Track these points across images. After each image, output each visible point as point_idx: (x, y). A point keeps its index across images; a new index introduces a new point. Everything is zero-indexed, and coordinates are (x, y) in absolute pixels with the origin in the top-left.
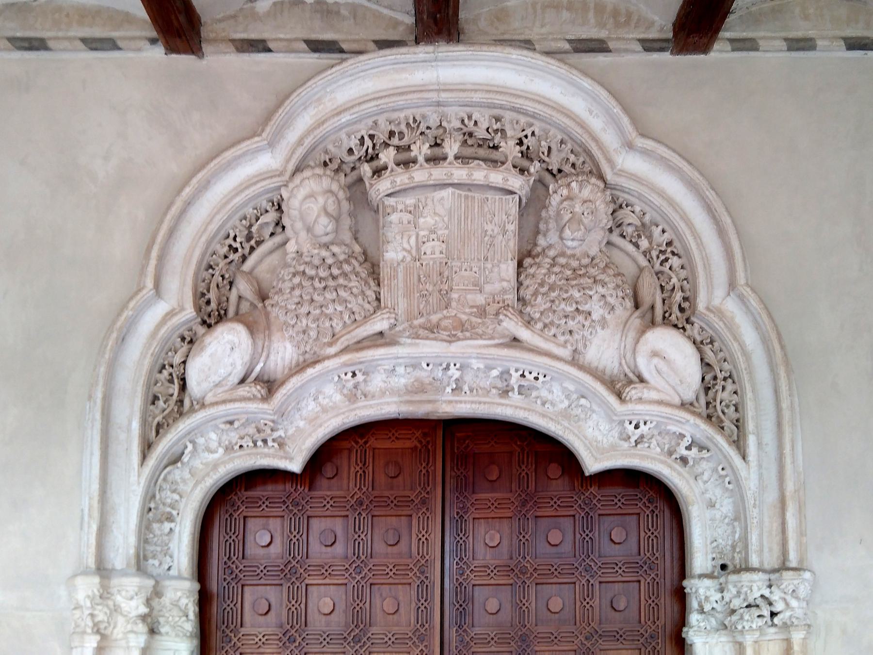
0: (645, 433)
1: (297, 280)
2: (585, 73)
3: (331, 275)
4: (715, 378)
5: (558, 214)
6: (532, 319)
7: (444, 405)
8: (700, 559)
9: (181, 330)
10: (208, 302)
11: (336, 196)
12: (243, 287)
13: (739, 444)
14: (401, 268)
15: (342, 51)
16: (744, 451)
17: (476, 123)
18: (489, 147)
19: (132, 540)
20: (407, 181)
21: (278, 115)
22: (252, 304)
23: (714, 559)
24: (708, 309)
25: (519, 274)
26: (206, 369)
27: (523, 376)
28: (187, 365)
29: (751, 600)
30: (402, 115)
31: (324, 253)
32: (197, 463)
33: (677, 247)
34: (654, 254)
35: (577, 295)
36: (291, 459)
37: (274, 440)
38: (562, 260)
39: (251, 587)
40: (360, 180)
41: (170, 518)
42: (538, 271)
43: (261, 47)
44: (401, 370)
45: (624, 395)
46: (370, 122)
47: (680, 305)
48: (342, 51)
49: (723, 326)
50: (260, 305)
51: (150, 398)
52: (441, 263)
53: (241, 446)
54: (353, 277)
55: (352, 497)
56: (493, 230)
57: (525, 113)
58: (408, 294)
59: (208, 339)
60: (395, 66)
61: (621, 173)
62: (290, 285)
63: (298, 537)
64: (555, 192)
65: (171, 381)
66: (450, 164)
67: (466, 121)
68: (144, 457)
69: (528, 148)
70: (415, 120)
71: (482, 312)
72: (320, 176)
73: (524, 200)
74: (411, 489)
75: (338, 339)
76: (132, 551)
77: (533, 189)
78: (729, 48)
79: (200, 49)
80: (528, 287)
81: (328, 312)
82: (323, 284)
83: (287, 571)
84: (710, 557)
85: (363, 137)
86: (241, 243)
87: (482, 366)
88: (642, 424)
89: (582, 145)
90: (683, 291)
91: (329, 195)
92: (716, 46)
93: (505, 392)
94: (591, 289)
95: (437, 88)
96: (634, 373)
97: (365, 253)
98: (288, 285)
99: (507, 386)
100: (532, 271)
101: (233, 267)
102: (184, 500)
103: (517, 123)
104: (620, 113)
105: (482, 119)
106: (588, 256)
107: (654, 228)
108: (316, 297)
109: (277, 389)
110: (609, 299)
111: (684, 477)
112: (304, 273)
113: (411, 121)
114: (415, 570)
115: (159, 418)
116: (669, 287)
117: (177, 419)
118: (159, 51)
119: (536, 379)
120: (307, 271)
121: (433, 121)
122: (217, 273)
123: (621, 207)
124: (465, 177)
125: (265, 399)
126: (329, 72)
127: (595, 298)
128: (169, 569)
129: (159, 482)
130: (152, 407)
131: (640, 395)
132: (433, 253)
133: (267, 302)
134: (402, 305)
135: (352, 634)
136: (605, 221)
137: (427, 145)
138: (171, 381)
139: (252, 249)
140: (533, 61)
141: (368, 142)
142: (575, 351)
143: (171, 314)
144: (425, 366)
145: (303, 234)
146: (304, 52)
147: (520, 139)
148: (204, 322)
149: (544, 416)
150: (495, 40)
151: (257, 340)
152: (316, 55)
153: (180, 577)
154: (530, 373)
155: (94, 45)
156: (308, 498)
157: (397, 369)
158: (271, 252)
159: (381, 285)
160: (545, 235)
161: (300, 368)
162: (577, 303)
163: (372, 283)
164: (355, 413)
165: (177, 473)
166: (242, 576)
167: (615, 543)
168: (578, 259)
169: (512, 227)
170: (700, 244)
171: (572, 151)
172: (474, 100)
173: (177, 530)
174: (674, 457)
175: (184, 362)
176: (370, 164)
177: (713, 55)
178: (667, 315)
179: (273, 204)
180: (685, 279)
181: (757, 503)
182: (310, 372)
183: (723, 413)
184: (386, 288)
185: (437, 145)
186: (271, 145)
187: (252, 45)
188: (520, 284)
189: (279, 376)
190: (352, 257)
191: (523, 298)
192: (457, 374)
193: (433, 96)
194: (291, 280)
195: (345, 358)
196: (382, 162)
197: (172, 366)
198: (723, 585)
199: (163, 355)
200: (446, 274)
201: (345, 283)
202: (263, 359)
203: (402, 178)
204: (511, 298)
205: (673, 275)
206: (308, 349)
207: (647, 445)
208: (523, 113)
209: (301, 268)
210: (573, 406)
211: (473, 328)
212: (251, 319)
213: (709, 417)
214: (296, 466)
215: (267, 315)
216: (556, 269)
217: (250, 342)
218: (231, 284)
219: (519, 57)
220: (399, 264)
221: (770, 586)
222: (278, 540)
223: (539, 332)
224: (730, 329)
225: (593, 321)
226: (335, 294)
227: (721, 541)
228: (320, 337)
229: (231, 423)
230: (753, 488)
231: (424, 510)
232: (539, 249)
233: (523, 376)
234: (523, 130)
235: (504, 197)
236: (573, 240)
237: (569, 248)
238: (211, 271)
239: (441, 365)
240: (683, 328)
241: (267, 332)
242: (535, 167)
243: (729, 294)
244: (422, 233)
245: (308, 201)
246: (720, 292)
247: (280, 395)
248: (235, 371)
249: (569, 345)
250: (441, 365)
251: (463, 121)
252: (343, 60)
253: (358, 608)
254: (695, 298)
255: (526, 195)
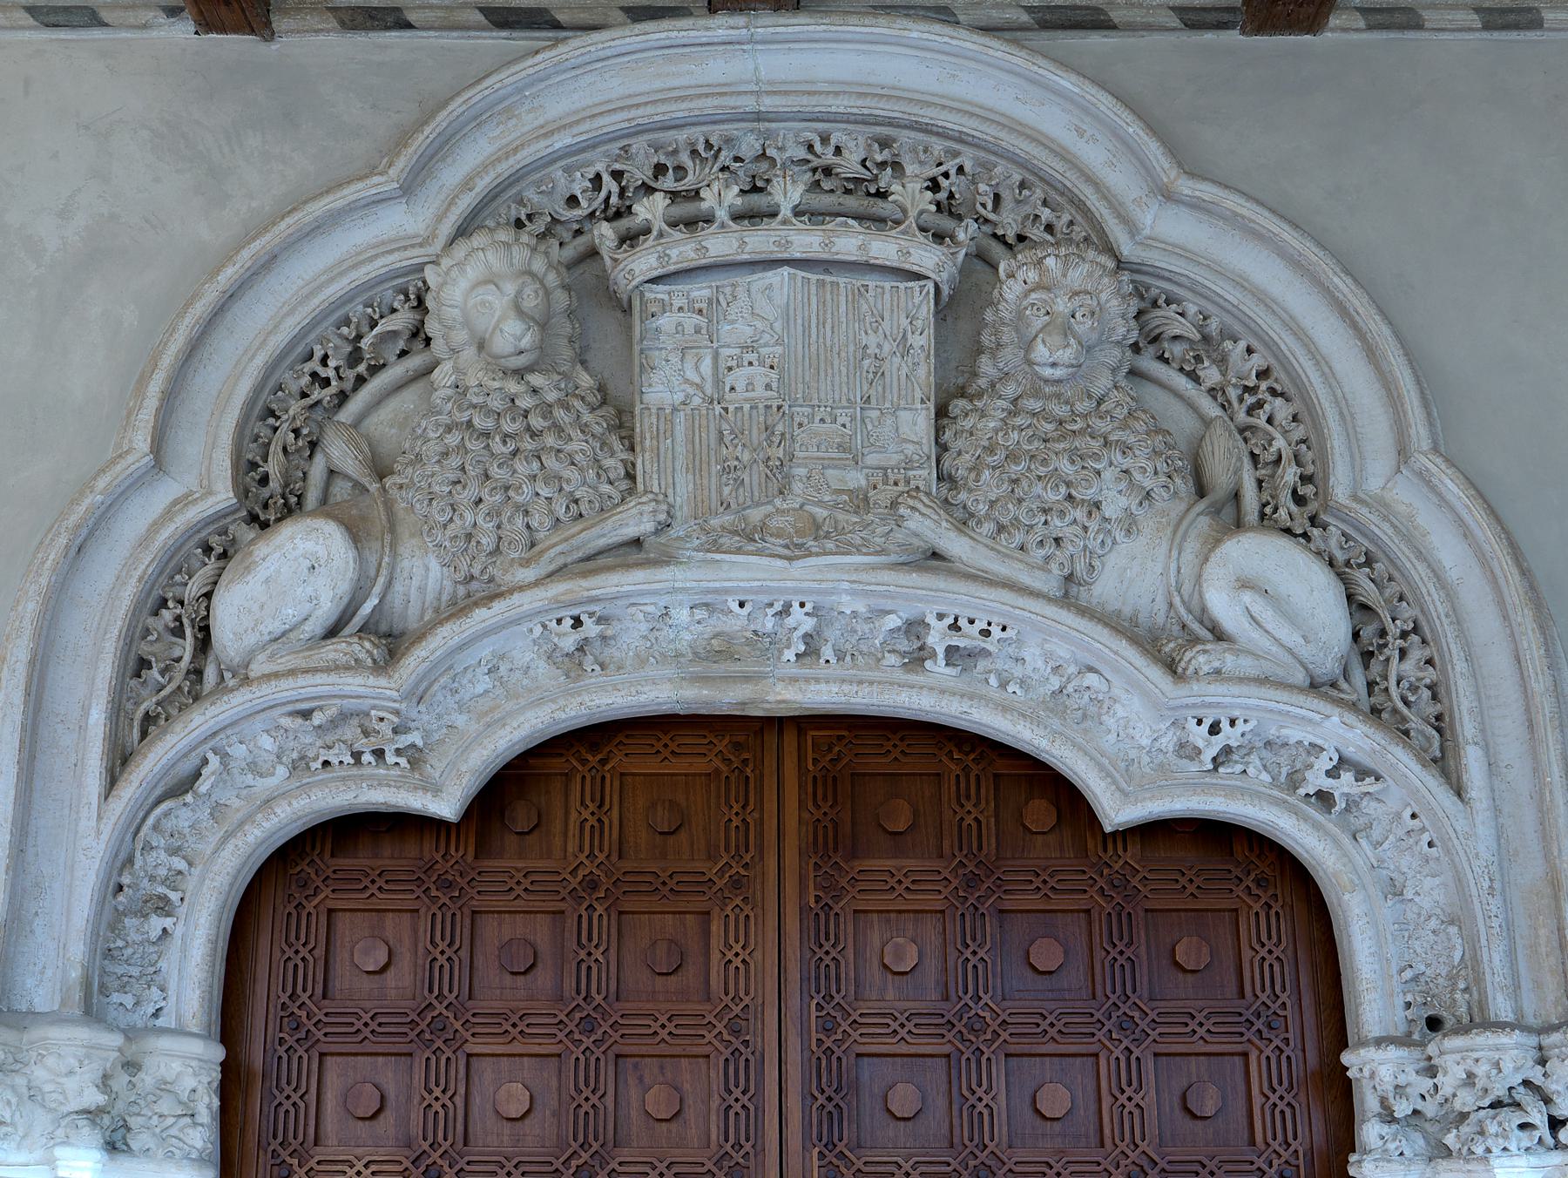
0: (1234, 744)
1: (453, 440)
2: (1063, 64)
3: (528, 428)
4: (1383, 633)
5: (1020, 315)
6: (972, 515)
7: (779, 687)
8: (1374, 1001)
9: (204, 534)
10: (264, 481)
11: (542, 283)
12: (339, 451)
13: (1445, 764)
14: (680, 418)
15: (557, 26)
16: (1459, 778)
17: (838, 151)
18: (869, 194)
19: (77, 950)
20: (693, 255)
21: (421, 138)
22: (357, 485)
23: (1408, 1005)
24: (1355, 498)
25: (939, 430)
26: (255, 608)
27: (955, 627)
28: (215, 599)
29: (1499, 1091)
30: (682, 136)
31: (513, 387)
32: (228, 797)
33: (1281, 380)
34: (1233, 394)
35: (1066, 467)
36: (436, 790)
37: (398, 752)
38: (1034, 404)
39: (339, 1059)
40: (593, 253)
41: (163, 907)
42: (981, 424)
43: (390, 19)
44: (682, 615)
45: (1183, 664)
46: (614, 148)
47: (1294, 492)
48: (557, 26)
49: (1390, 532)
50: (374, 487)
51: (132, 664)
52: (768, 407)
53: (326, 763)
54: (576, 434)
55: (573, 872)
56: (879, 346)
57: (942, 134)
58: (696, 466)
59: (261, 549)
60: (666, 51)
61: (1150, 242)
62: (439, 449)
63: (449, 952)
64: (1011, 276)
65: (178, 632)
66: (784, 222)
67: (818, 148)
68: (112, 780)
69: (951, 196)
70: (709, 146)
71: (860, 501)
72: (507, 245)
73: (946, 290)
74: (709, 858)
75: (542, 552)
76: (75, 974)
77: (964, 271)
78: (1362, 24)
79: (268, 24)
80: (959, 453)
81: (519, 499)
82: (511, 446)
83: (423, 1025)
84: (1399, 1001)
85: (598, 177)
86: (337, 369)
87: (861, 608)
88: (1225, 725)
89: (1063, 191)
90: (1299, 464)
91: (528, 279)
92: (1334, 21)
93: (918, 659)
94: (1096, 457)
95: (756, 88)
96: (1201, 622)
97: (601, 388)
98: (432, 449)
99: (921, 648)
100: (968, 423)
101: (318, 415)
102: (196, 871)
103: (925, 151)
104: (1141, 133)
105: (852, 144)
106: (1090, 397)
107: (1228, 344)
108: (495, 471)
109: (407, 649)
110: (1137, 476)
111: (1327, 833)
112: (469, 424)
113: (701, 148)
114: (720, 1027)
115: (148, 704)
116: (1269, 457)
117: (187, 706)
118: (182, 31)
119: (986, 633)
120: (476, 421)
121: (749, 146)
122: (285, 426)
123: (1155, 304)
124: (816, 247)
125: (380, 668)
126: (530, 62)
127: (1108, 475)
128: (156, 1014)
129: (142, 834)
130: (134, 682)
131: (1216, 664)
132: (750, 386)
133: (388, 482)
134: (683, 490)
135: (574, 1163)
136: (1122, 330)
137: (736, 189)
138: (178, 632)
139: (361, 381)
140: (954, 42)
141: (609, 184)
142: (1069, 578)
143: (184, 501)
144: (735, 606)
145: (469, 353)
146: (483, 29)
147: (934, 180)
148: (253, 518)
149: (1005, 709)
150: (874, 7)
151: (367, 552)
152: (504, 34)
153: (180, 1032)
154: (972, 622)
155: (52, 19)
156: (473, 874)
157: (672, 612)
158: (399, 387)
159: (638, 449)
160: (994, 357)
161: (457, 608)
162: (1068, 484)
163: (617, 446)
164: (579, 700)
165: (182, 815)
166: (319, 1035)
167: (1185, 971)
168: (1067, 403)
169: (922, 341)
170: (1329, 376)
171: (1045, 203)
172: (833, 109)
173: (178, 932)
174: (1302, 791)
175: (208, 595)
176: (615, 224)
177: (1327, 38)
178: (1268, 510)
179: (407, 299)
180: (1303, 441)
181: (1497, 885)
182: (481, 617)
183: (1406, 702)
184: (647, 455)
185: (755, 189)
186: (408, 189)
187: (372, 18)
188: (942, 448)
189: (413, 624)
190: (576, 396)
191: (950, 476)
192: (808, 624)
193: (749, 104)
194: (441, 438)
195: (558, 588)
196: (639, 220)
197: (182, 603)
198: (1435, 1061)
199: (163, 580)
200: (780, 428)
201: (557, 444)
202: (377, 589)
203: (682, 250)
204: (925, 475)
205: (1277, 435)
206: (476, 571)
207: (1239, 768)
208: (938, 134)
209: (465, 417)
210: (1070, 689)
211: (842, 532)
212: (354, 512)
213: (1375, 711)
214: (447, 806)
215: (389, 506)
216: (1018, 421)
217: (351, 554)
218: (313, 445)
219: (925, 36)
220: (675, 409)
221: (1542, 1062)
222: (404, 962)
223: (989, 542)
224: (1408, 538)
225: (1106, 520)
226: (535, 465)
227: (1423, 968)
228: (504, 547)
229: (306, 715)
230: (1485, 854)
231: (738, 901)
232: (982, 382)
233: (955, 627)
234: (940, 164)
235: (902, 286)
236: (1054, 365)
237: (1046, 381)
238: (271, 421)
239: (771, 605)
240: (1305, 535)
241: (388, 538)
242: (966, 232)
243: (1399, 471)
244: (725, 352)
245: (481, 290)
246: (1378, 467)
247: (414, 662)
248: (319, 612)
249: (1054, 567)
250: (771, 605)
251: (810, 148)
252: (557, 42)
253: (586, 1107)
254: (1326, 479)
255: (950, 281)
